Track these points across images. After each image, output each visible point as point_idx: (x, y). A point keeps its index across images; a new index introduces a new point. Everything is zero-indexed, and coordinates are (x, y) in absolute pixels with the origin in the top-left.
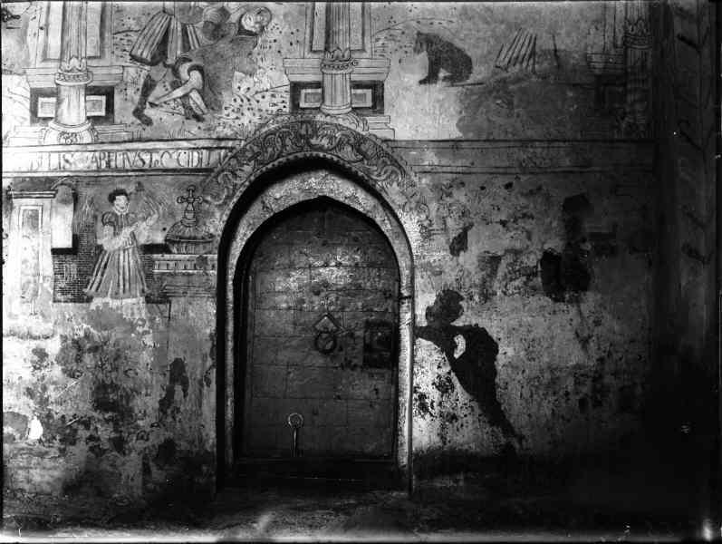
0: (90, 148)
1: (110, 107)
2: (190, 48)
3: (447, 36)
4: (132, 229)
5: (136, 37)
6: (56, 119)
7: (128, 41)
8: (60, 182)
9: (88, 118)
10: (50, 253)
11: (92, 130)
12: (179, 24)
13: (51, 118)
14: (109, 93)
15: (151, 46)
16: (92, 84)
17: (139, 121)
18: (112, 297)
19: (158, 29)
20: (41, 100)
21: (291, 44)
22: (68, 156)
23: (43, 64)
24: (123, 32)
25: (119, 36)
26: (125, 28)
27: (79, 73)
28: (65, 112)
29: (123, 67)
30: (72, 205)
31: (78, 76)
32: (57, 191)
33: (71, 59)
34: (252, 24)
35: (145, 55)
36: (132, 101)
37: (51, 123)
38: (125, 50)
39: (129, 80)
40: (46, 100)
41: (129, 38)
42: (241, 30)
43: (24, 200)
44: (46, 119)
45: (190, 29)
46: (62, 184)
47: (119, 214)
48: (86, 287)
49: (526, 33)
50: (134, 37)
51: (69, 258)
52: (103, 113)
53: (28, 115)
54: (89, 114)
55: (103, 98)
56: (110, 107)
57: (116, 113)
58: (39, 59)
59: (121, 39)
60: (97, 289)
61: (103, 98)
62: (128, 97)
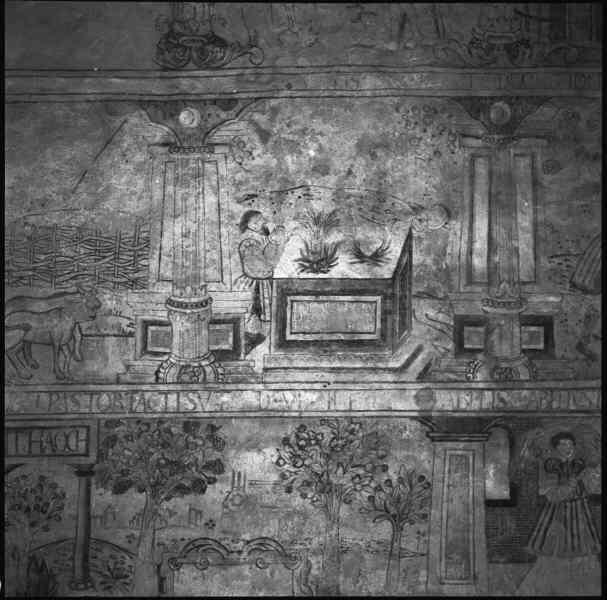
0: (527, 385)
1: (549, 338)
4: (578, 478)
6: (487, 350)
7: (568, 266)
8: (493, 423)
9: (524, 351)
10: (483, 506)
11: (530, 365)
13: (479, 351)
14: (546, 323)
16: (525, 313)
17: (582, 356)
18: (558, 556)
20: (466, 329)
22: (504, 394)
23: (468, 288)
24: (562, 255)
25: (556, 260)
27: (510, 300)
28: (497, 348)
29: (562, 294)
30: (508, 449)
31: (509, 303)
32: (490, 433)
33: (501, 283)
35: (587, 282)
36: (574, 333)
37: (480, 357)
39: (567, 309)
40: (471, 329)
41: (568, 263)
43: (449, 444)
44: (473, 351)
46: (496, 426)
47: (564, 460)
48: (527, 544)
50: (574, 262)
51: (506, 510)
52: (541, 346)
53: (451, 346)
54: (524, 347)
55: (541, 330)
56: (549, 338)
57: (557, 347)
58: (464, 282)
59: (560, 264)
60: (541, 548)
61: (541, 330)
62: (569, 330)
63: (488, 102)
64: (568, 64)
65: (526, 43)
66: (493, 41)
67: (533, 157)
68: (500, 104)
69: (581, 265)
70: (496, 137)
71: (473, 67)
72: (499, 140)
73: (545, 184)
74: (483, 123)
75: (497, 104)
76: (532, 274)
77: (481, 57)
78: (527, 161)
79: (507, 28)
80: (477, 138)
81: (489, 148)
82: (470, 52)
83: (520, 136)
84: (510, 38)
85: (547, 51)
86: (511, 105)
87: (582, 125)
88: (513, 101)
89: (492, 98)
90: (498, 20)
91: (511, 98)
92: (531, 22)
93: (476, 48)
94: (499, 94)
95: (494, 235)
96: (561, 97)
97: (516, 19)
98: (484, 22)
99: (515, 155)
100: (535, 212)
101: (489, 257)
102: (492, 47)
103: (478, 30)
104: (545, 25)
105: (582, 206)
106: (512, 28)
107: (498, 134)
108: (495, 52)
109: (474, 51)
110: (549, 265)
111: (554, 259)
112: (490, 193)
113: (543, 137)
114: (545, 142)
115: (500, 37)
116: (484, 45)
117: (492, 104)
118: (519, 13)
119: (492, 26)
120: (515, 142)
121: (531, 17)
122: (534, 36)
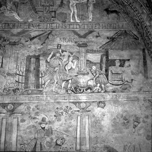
2: (42, 149)
3: (111, 146)
5: (27, 146)
7: (25, 147)
12: (39, 143)
15: (31, 149)
19: (33, 144)
21: (70, 148)
25: (22, 145)
26: (24, 143)
34: (60, 142)
38: (23, 150)
41: (25, 146)
42: (57, 144)
45: (42, 143)
49: (132, 145)
50: (26, 146)
59: (23, 146)
63: (7, 104)
64: (29, 94)
65: (18, 89)
66: (9, 89)
67: (18, 118)
68: (10, 104)
69: (28, 146)
70: (9, 113)
71: (4, 95)
72: (9, 114)
73: (21, 125)
74: (6, 109)
75: (9, 105)
76: (15, 149)
77: (6, 93)
78: (16, 119)
79: (13, 85)
80: (4, 113)
81: (7, 116)
82: (4, 91)
83: (14, 113)
84: (14, 88)
85: (23, 91)
86: (13, 105)
87: (31, 109)
88: (14, 104)
89: (8, 103)
90: (11, 83)
91: (13, 103)
92: (20, 83)
93: (5, 90)
94: (10, 102)
95: (6, 139)
96: (26, 103)
97: (16, 83)
98: (7, 83)
99: (13, 118)
100: (17, 132)
101: (5, 145)
102: (9, 90)
103: (6, 86)
104: (23, 84)
105: (29, 131)
106: (14, 85)
107: (9, 112)
108: (10, 91)
109: (5, 91)
110: (20, 147)
111: (21, 145)
112: (6, 128)
113: (21, 113)
114: (21, 115)
115: (11, 88)
116: (7, 90)
117: (8, 105)
118: (17, 81)
119: (10, 85)
120: (13, 115)
121: (20, 82)
122: (20, 87)
